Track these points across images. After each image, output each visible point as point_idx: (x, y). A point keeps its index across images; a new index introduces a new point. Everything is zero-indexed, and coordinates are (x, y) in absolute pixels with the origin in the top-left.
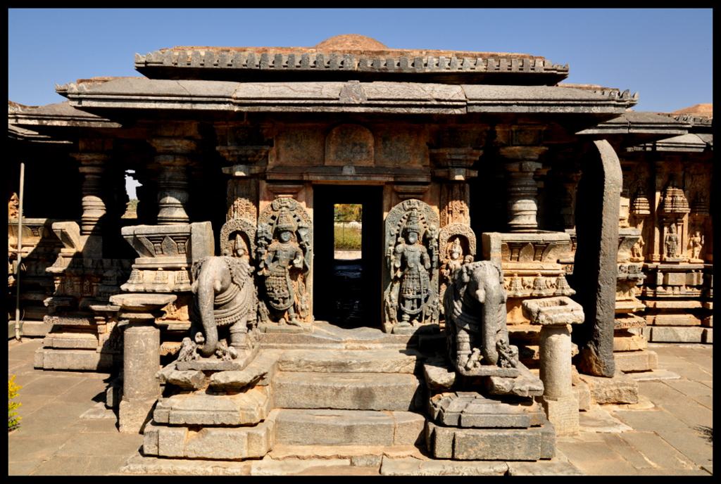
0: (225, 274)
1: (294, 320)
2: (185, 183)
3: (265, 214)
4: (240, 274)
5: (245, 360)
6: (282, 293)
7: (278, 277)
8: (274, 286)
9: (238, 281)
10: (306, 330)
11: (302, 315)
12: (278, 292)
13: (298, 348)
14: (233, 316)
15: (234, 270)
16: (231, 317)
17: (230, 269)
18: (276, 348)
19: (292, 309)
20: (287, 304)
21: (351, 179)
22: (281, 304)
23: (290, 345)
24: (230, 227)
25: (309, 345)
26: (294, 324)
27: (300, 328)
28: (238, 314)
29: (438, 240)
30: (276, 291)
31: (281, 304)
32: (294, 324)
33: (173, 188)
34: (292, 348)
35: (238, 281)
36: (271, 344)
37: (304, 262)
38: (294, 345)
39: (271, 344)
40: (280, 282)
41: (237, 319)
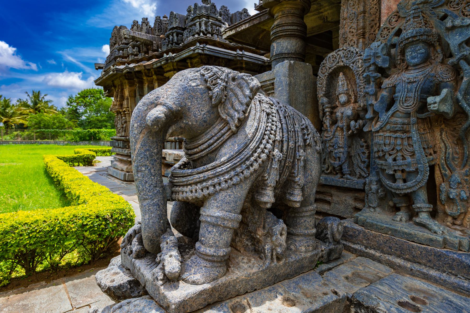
0: (191, 98)
1: (424, 217)
2: (296, 28)
3: (385, 32)
4: (233, 99)
5: (200, 288)
6: (400, 162)
7: (396, 132)
8: (387, 148)
9: (228, 114)
10: (445, 243)
11: (448, 211)
12: (395, 160)
13: (426, 277)
14: (199, 186)
16: (194, 187)
17: (209, 89)
18: (380, 261)
19: (423, 195)
20: (409, 184)
22: (400, 184)
23: (409, 265)
24: (328, 65)
25: (453, 279)
26: (424, 226)
27: (433, 237)
28: (210, 182)
30: (390, 160)
31: (400, 184)
32: (424, 226)
33: (280, 37)
34: (412, 273)
35: (228, 114)
36: (372, 252)
37: (457, 101)
38: (416, 267)
39: (372, 252)
40: (399, 142)
41: (206, 192)
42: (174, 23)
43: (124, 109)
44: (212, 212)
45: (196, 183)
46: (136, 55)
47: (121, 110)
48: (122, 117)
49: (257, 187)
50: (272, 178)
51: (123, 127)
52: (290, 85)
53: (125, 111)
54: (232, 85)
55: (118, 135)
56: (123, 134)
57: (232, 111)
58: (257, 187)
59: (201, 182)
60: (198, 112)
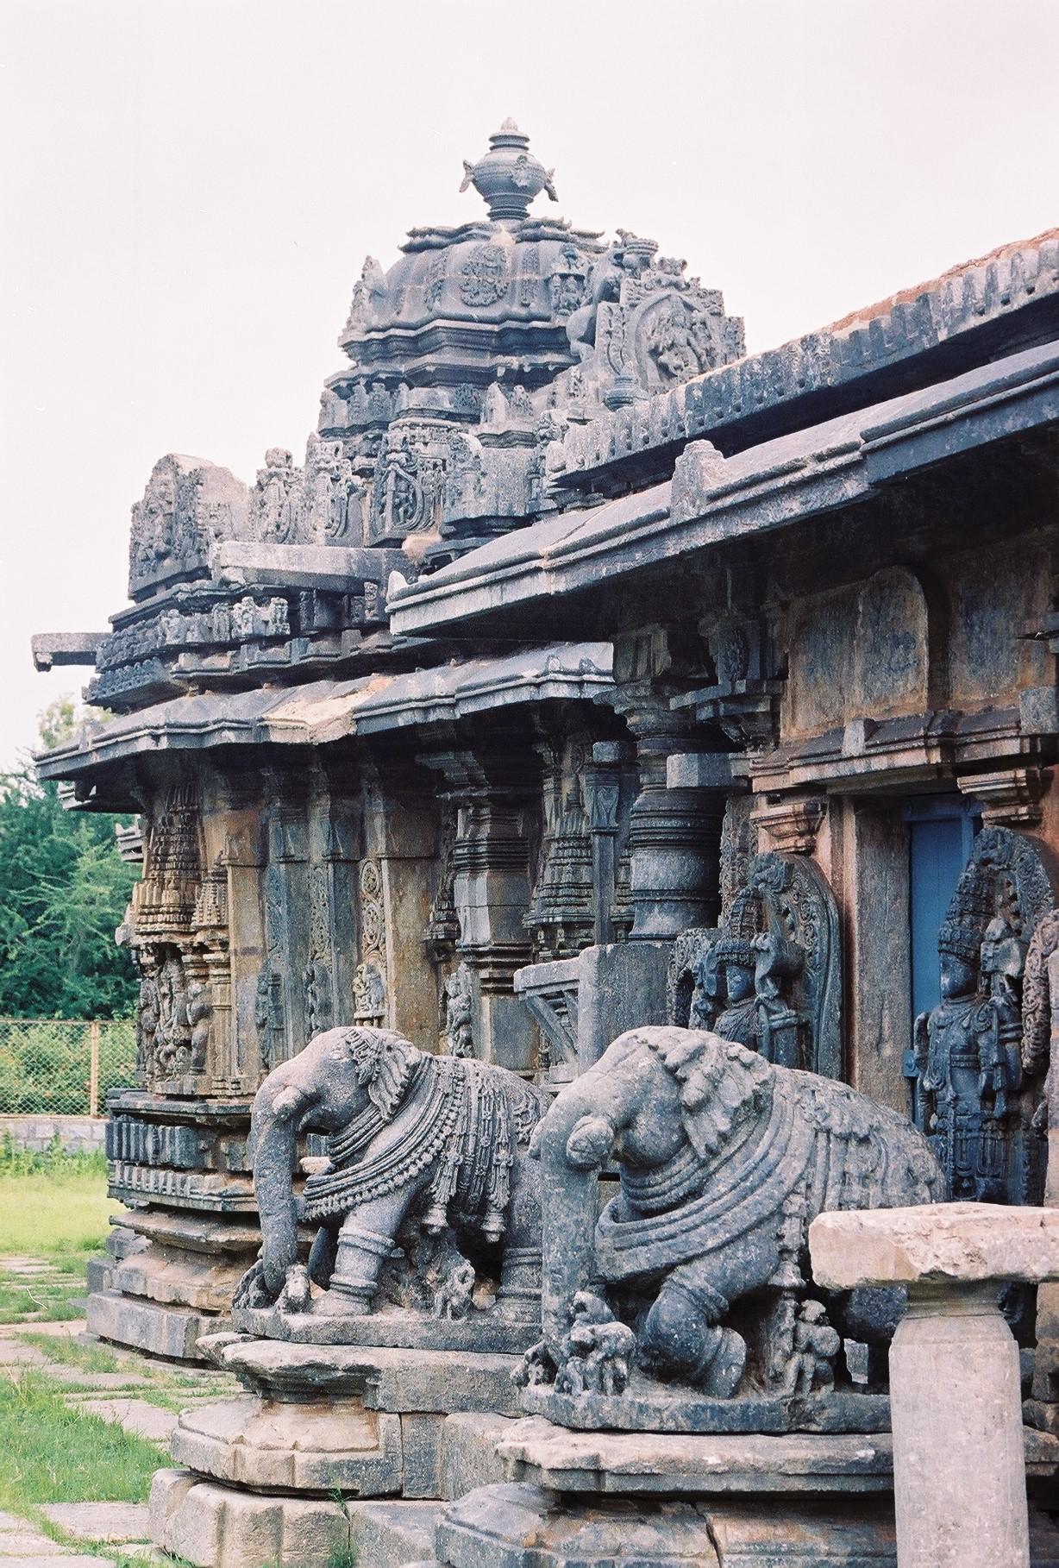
2: (674, 823)
9: (380, 1098)
15: (364, 1066)
17: (355, 1062)
21: (860, 767)
28: (349, 1191)
29: (1016, 983)
35: (380, 1098)
41: (343, 1204)
42: (469, 495)
43: (200, 938)
44: (351, 1230)
45: (332, 1193)
46: (278, 640)
47: (180, 941)
48: (184, 983)
49: (418, 1204)
50: (443, 1190)
51: (187, 1043)
52: (600, 1002)
53: (202, 949)
54: (387, 1055)
55: (159, 1087)
56: (188, 1083)
57: (385, 1095)
58: (418, 1204)
59: (338, 1191)
60: (341, 1095)
